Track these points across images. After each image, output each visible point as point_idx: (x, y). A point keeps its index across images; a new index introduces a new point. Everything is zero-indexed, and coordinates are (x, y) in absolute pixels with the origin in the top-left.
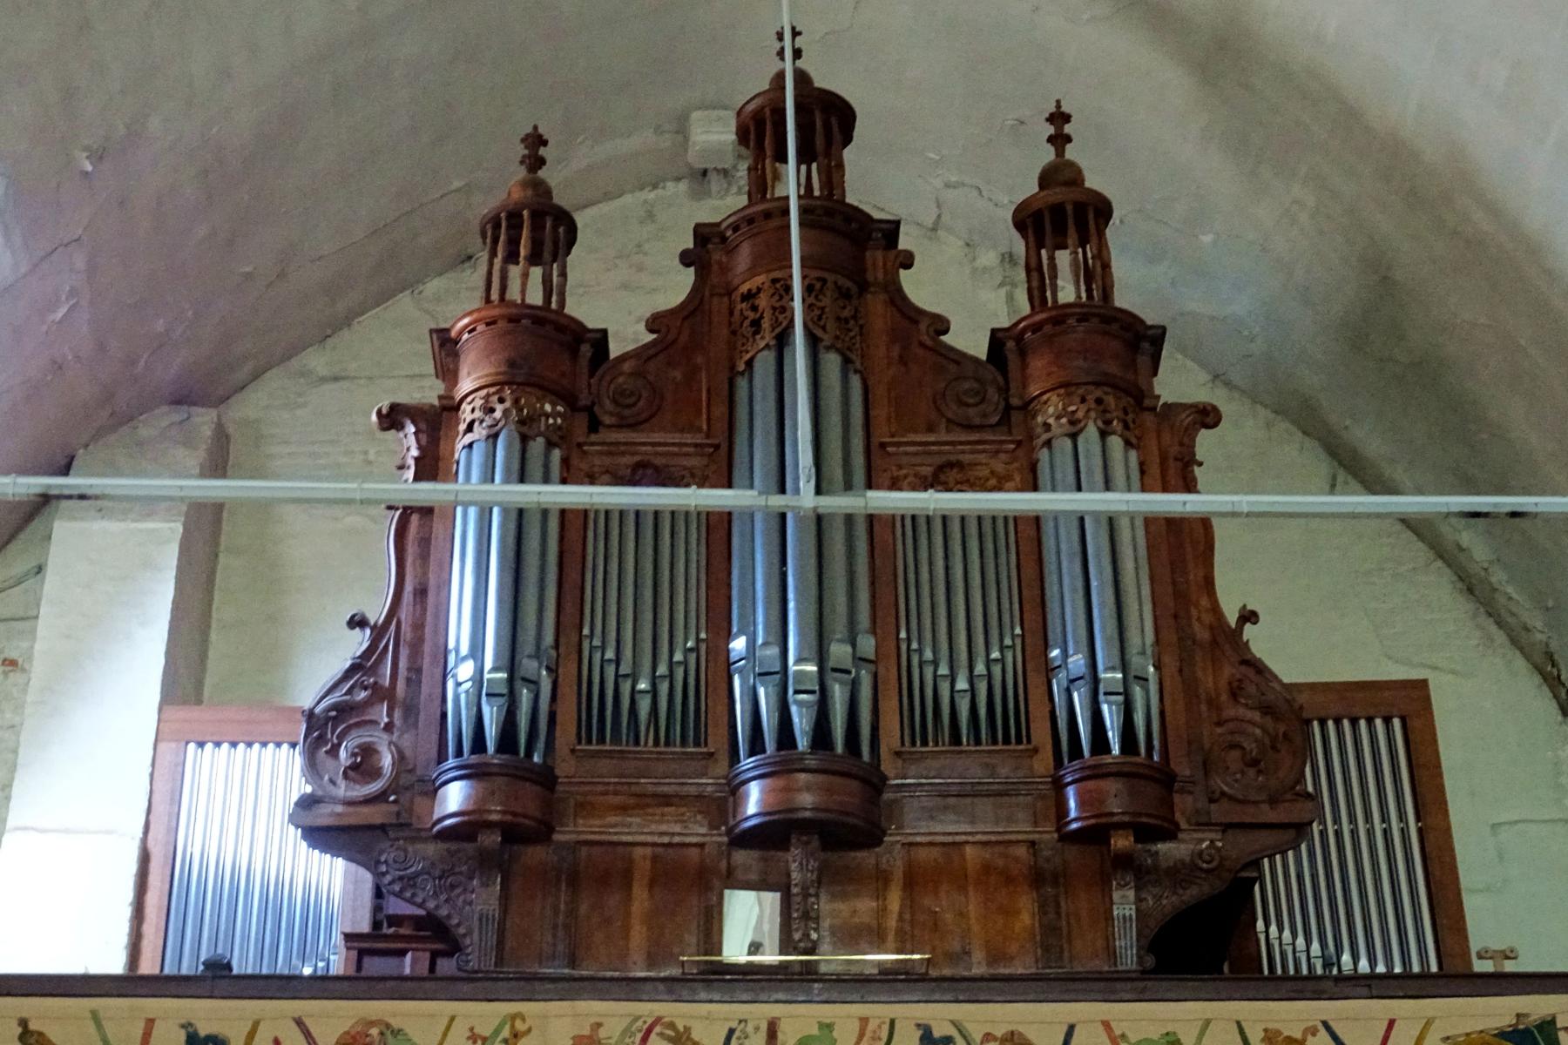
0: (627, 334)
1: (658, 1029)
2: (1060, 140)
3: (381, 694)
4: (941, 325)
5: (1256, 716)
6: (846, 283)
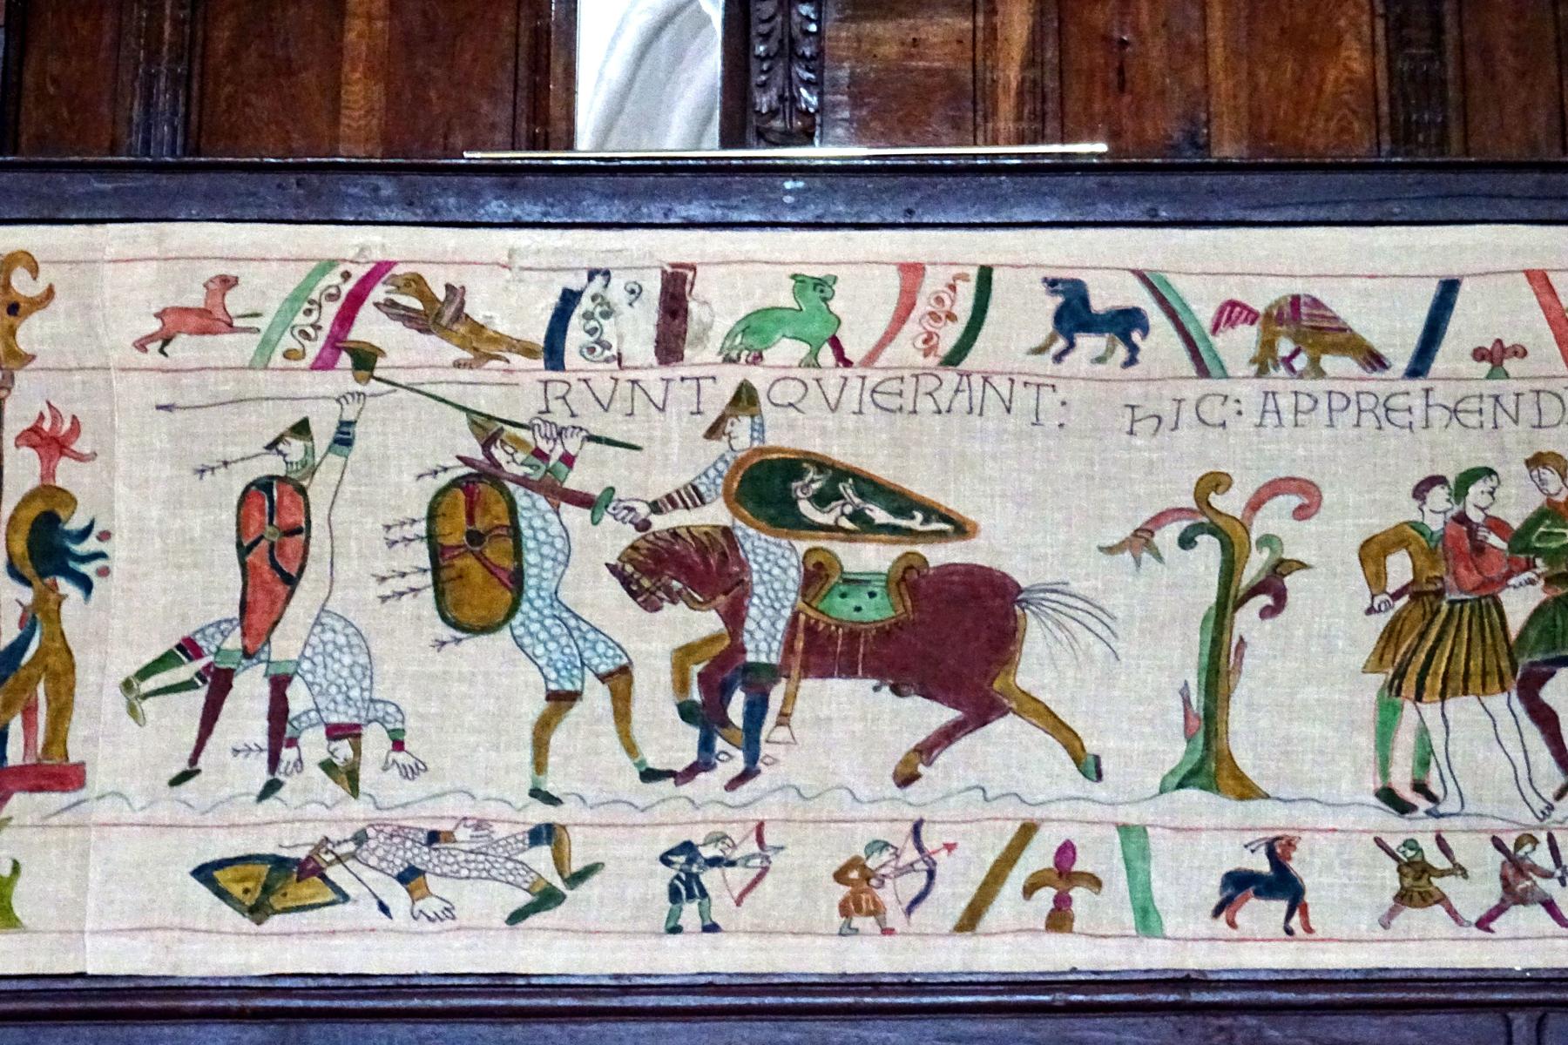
1: (379, 293)
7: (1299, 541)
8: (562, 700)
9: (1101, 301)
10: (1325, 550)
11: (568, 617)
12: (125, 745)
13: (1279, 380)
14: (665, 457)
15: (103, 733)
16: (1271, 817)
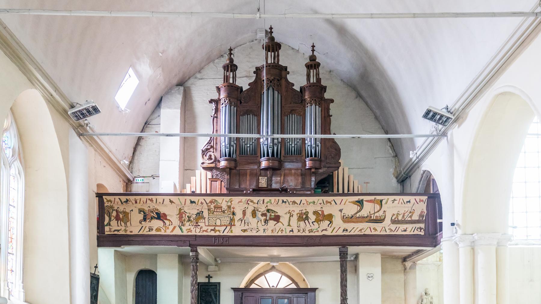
0: (246, 87)
2: (313, 51)
3: (212, 147)
4: (293, 85)
6: (278, 78)
10: (295, 214)
12: (237, 223)
14: (263, 209)
15: (236, 223)
16: (292, 228)
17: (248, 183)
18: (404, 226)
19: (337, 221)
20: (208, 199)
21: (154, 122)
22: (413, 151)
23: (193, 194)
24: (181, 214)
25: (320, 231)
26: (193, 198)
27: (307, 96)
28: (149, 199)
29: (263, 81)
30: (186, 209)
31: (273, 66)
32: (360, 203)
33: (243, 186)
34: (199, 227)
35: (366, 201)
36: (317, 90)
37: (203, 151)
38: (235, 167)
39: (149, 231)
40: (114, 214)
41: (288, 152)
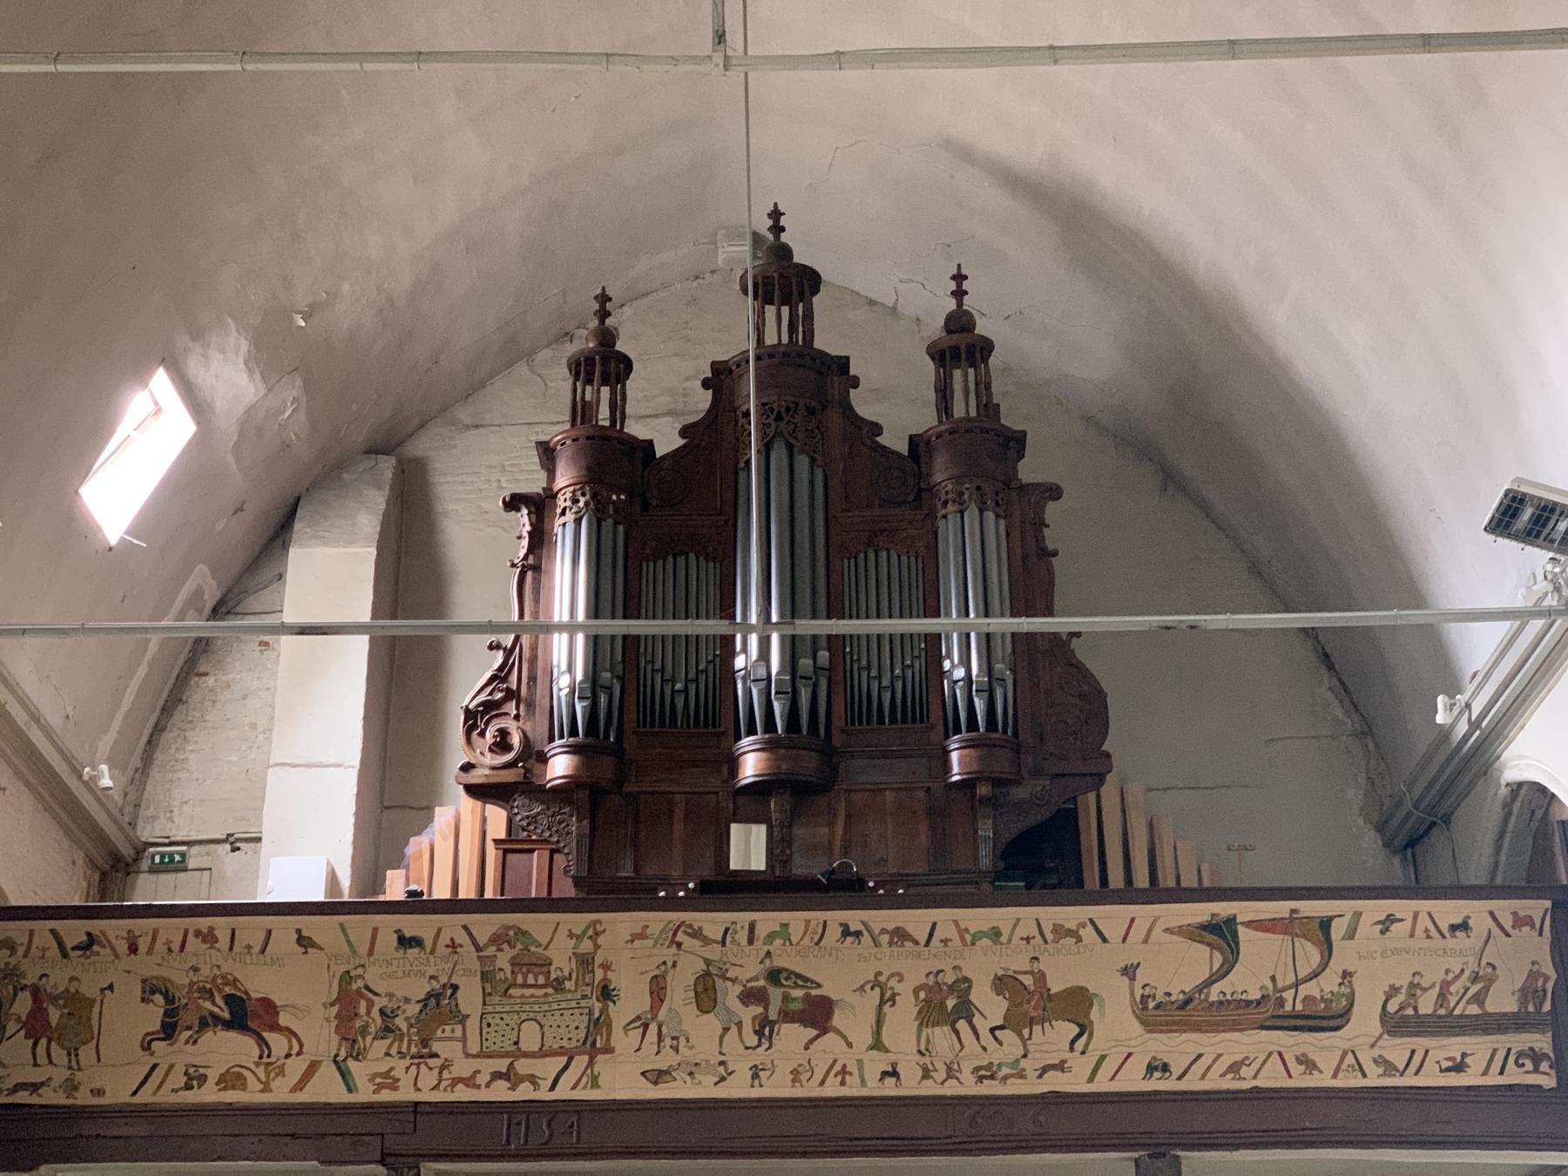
0: (667, 441)
4: (877, 429)
5: (1076, 700)
7: (899, 988)
8: (726, 1030)
9: (852, 929)
10: (905, 990)
11: (727, 1010)
13: (894, 948)
14: (749, 969)
16: (892, 1057)
17: (677, 851)
18: (1454, 1046)
19: (1115, 1021)
20: (486, 926)
21: (253, 603)
22: (1452, 697)
23: (416, 903)
24: (347, 999)
25: (1032, 1075)
26: (413, 924)
27: (941, 472)
28: (198, 933)
29: (747, 414)
30: (373, 976)
31: (786, 355)
32: (1222, 934)
33: (651, 869)
34: (433, 1062)
35: (1248, 924)
36: (986, 448)
37: (469, 714)
38: (619, 783)
39: (188, 1087)
40: (23, 1004)
41: (862, 712)
